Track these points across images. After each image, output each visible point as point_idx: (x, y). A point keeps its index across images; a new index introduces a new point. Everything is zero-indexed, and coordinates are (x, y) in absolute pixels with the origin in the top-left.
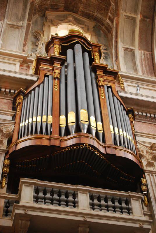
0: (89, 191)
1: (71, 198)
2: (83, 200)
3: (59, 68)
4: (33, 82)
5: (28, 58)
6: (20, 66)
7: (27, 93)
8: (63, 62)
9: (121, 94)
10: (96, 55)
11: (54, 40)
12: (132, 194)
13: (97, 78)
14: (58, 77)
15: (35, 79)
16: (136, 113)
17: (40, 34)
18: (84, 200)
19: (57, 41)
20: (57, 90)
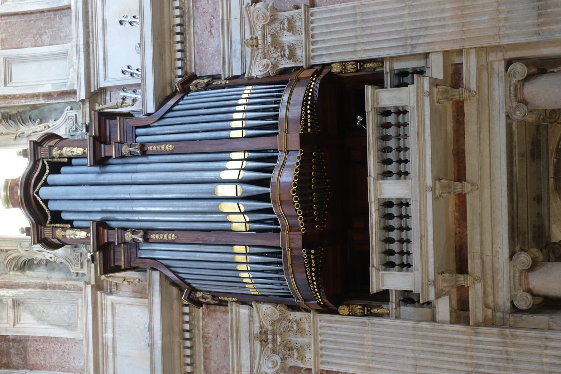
0: (376, 179)
1: (394, 210)
2: (392, 189)
3: (120, 234)
4: (164, 277)
5: (93, 282)
6: (111, 293)
7: (187, 287)
8: (102, 225)
9: (151, 108)
10: (59, 152)
11: (43, 237)
12: (369, 107)
13: (123, 157)
14: (141, 234)
15: (156, 275)
16: (180, 72)
17: (13, 259)
18: (392, 189)
19: (47, 233)
20: (173, 235)
